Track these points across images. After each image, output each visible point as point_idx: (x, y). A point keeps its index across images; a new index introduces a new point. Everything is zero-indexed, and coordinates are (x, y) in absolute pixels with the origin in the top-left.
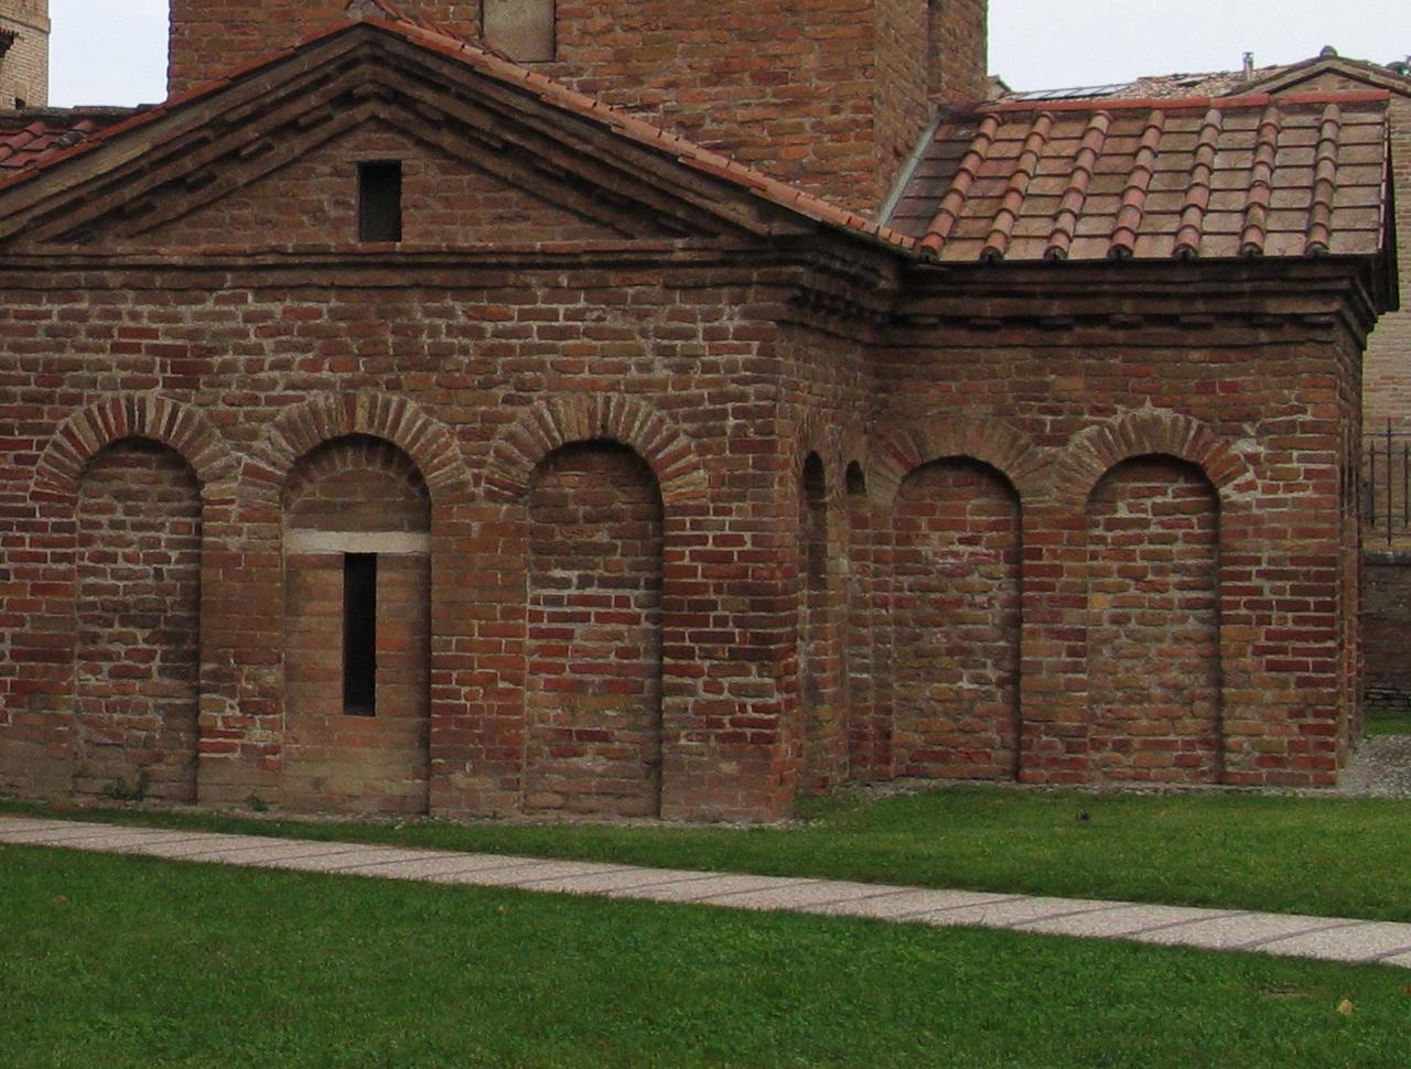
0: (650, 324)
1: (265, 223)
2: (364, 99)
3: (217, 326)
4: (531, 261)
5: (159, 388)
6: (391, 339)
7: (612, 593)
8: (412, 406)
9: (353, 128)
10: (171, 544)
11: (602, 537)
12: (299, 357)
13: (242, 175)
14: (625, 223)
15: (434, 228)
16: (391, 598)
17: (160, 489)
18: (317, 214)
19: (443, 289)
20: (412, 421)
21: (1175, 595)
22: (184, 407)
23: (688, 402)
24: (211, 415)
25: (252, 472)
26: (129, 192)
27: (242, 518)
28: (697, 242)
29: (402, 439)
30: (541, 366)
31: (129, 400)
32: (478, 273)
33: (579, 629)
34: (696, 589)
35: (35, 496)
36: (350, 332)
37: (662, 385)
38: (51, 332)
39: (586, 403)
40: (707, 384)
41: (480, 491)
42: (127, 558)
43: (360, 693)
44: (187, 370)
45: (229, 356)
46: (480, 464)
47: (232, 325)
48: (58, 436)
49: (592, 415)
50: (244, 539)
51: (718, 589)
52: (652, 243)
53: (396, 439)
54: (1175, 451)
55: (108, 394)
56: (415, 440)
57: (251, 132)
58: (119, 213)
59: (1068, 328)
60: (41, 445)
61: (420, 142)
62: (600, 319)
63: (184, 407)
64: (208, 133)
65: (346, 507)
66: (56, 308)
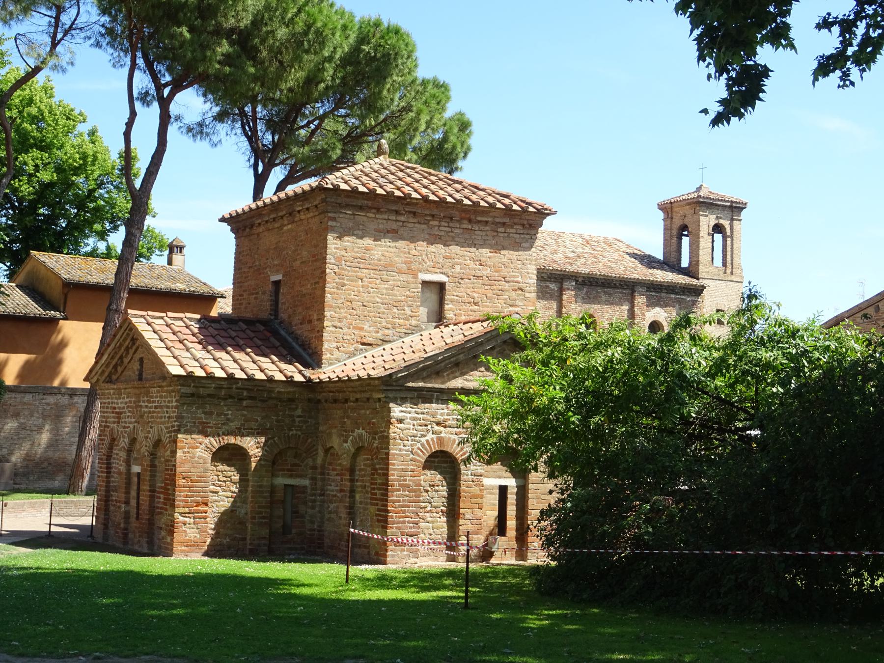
9: (138, 348)
13: (126, 361)
57: (123, 349)
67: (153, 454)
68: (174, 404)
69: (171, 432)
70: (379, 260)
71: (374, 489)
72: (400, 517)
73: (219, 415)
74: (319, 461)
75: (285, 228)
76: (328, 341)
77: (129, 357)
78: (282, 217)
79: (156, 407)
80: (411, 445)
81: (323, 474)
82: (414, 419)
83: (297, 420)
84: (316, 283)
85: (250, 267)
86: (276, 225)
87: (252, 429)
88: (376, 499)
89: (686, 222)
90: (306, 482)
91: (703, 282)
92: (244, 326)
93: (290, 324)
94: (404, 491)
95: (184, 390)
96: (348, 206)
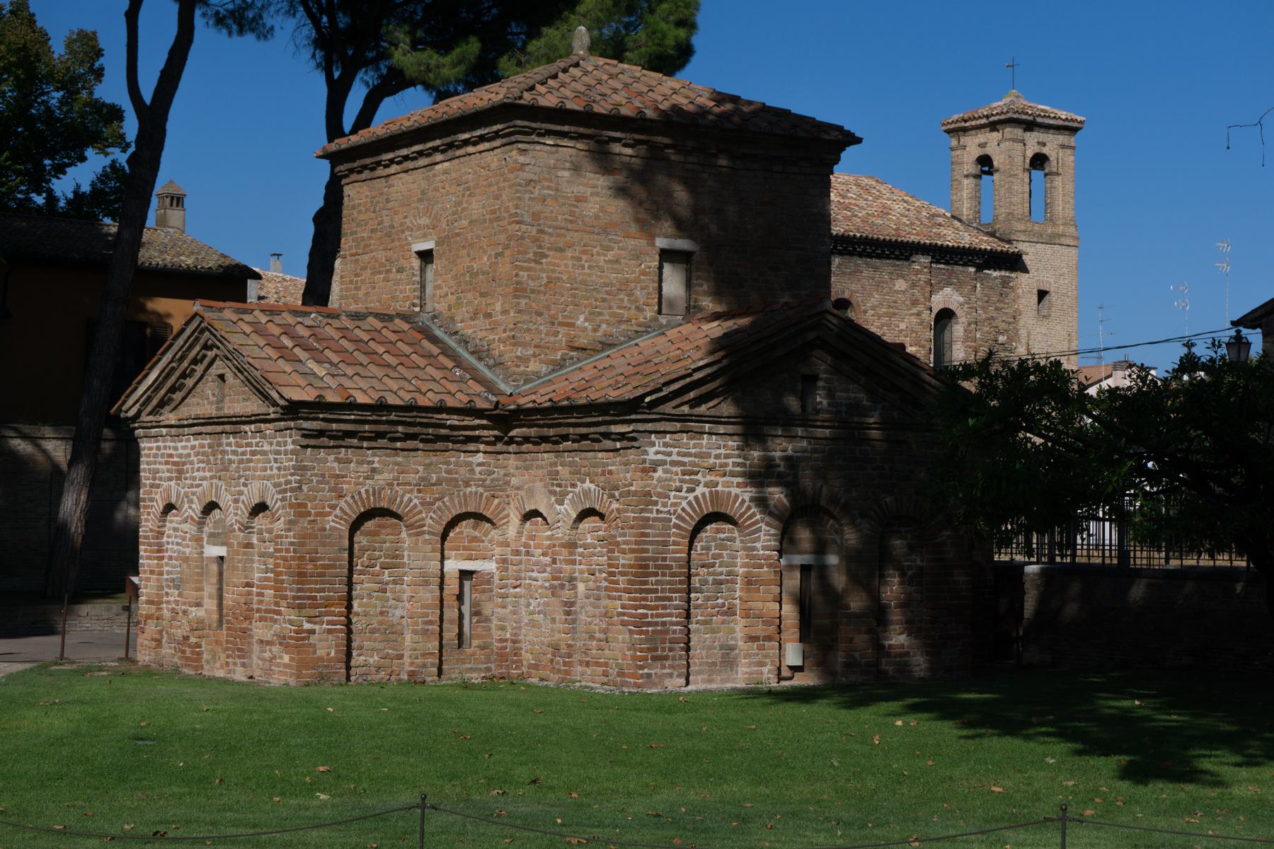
3: (185, 452)
13: (189, 382)
23: (279, 485)
24: (186, 495)
25: (192, 518)
32: (235, 423)
34: (281, 573)
35: (151, 530)
38: (156, 456)
46: (236, 514)
57: (185, 364)
64: (174, 364)
67: (246, 528)
68: (290, 447)
69: (285, 491)
70: (597, 217)
71: (612, 574)
72: (658, 616)
73: (360, 463)
74: (512, 531)
75: (438, 167)
76: (525, 345)
78: (435, 149)
79: (254, 453)
80: (673, 505)
81: (517, 553)
82: (673, 463)
83: (478, 469)
84: (497, 255)
85: (373, 231)
86: (423, 161)
87: (409, 484)
88: (617, 590)
89: (988, 150)
90: (489, 566)
91: (1022, 247)
92: (378, 324)
93: (452, 318)
94: (664, 575)
95: (306, 424)
96: (549, 133)
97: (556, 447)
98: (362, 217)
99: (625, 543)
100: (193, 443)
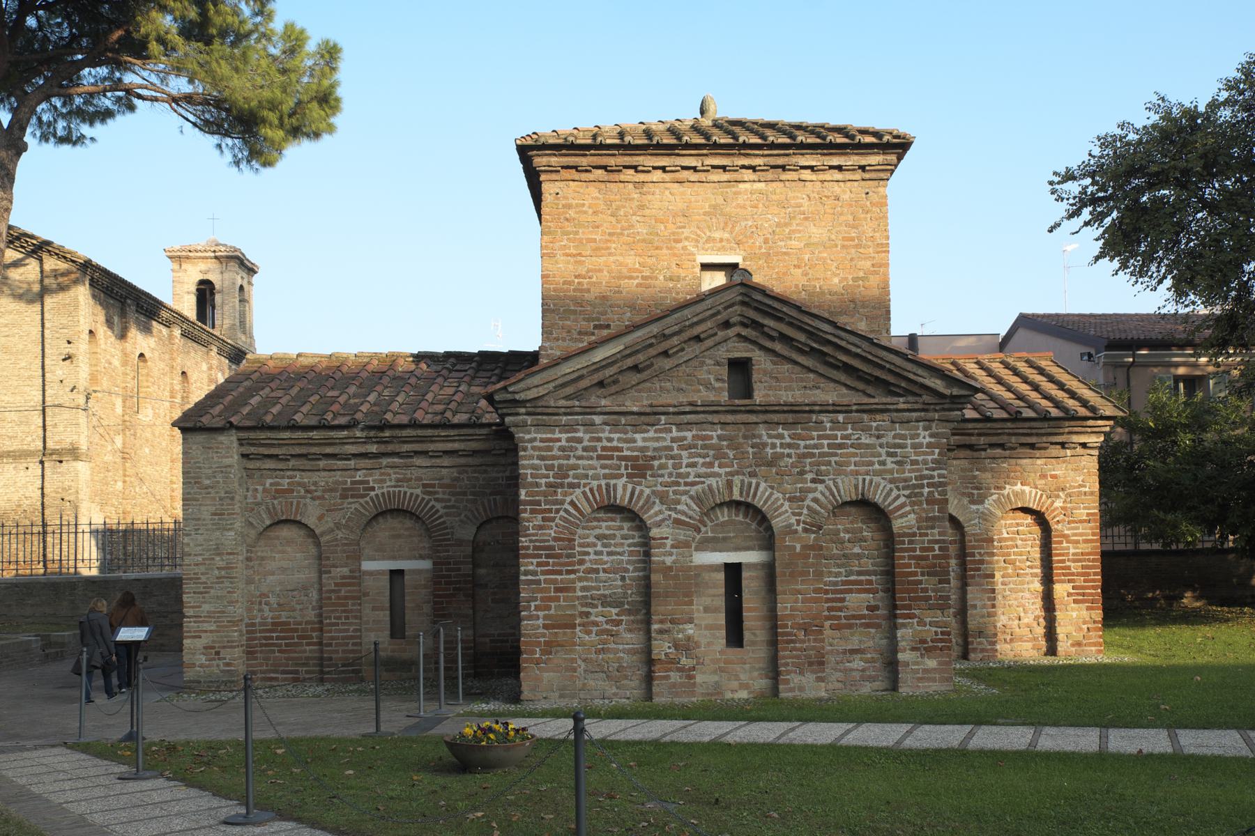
0: (884, 440)
1: (680, 390)
2: (734, 325)
3: (656, 445)
4: (826, 409)
5: (625, 479)
6: (751, 450)
7: (862, 578)
8: (763, 485)
10: (629, 562)
11: (857, 550)
12: (701, 460)
13: (667, 363)
14: (870, 390)
15: (770, 392)
16: (751, 585)
17: (622, 532)
18: (708, 385)
19: (778, 424)
20: (763, 493)
21: (1029, 571)
22: (638, 488)
23: (905, 480)
24: (653, 492)
25: (677, 522)
26: (608, 372)
27: (673, 546)
28: (910, 399)
29: (758, 502)
30: (829, 463)
31: (608, 485)
32: (796, 414)
33: (848, 596)
34: (915, 574)
35: (555, 539)
36: (728, 447)
37: (891, 472)
38: (562, 449)
39: (853, 482)
40: (910, 471)
41: (800, 528)
42: (605, 571)
43: (735, 635)
44: (640, 468)
45: (663, 461)
46: (800, 514)
47: (665, 444)
48: (567, 506)
49: (856, 487)
50: (674, 557)
51: (923, 575)
52: (884, 400)
53: (755, 503)
54: (1031, 506)
55: (595, 483)
56: (766, 502)
57: (675, 340)
58: (601, 384)
59: (985, 450)
60: (557, 511)
61: (762, 348)
62: (859, 439)
63: (638, 488)
64: (653, 340)
65: (724, 539)
66: (564, 436)
71: (1063, 561)
77: (684, 356)
79: (840, 446)
97: (976, 454)
98: (583, 218)
99: (1075, 535)
100: (675, 433)
